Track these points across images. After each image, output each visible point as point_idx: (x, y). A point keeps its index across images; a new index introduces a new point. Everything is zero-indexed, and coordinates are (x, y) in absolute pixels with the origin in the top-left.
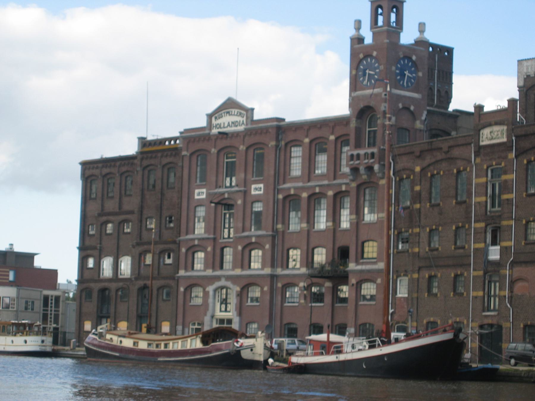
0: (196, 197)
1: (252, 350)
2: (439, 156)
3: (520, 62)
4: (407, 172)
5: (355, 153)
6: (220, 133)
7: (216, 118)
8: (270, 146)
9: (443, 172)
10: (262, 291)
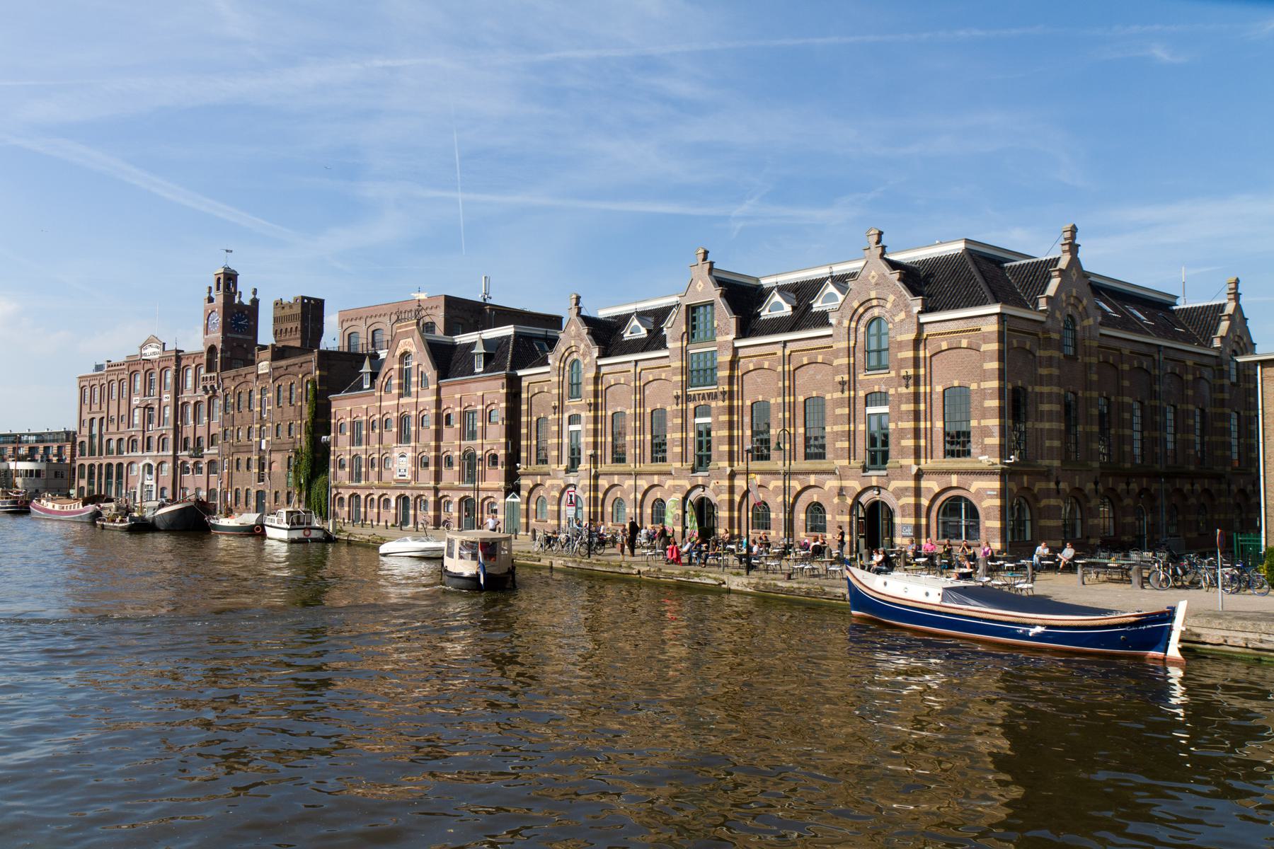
2: (242, 379)
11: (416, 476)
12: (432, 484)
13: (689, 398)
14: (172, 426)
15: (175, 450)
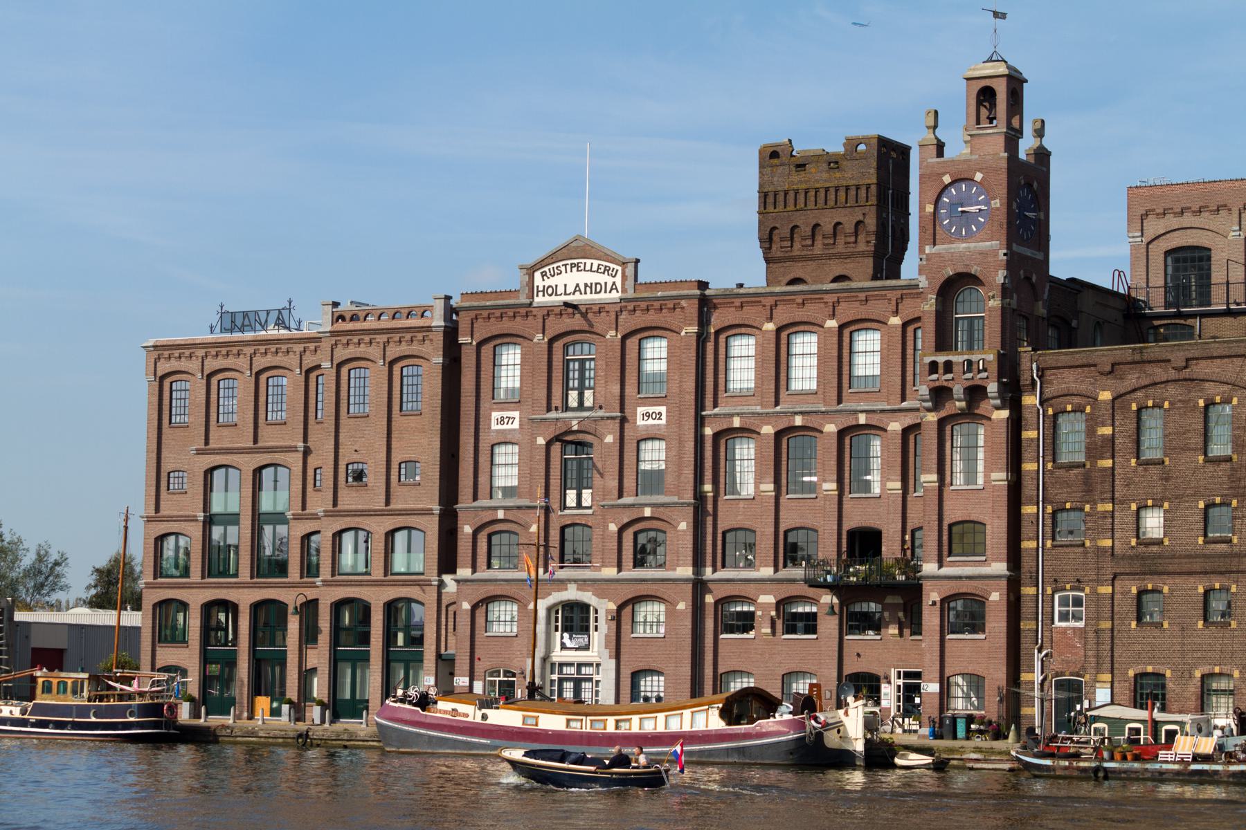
0: (494, 426)
1: (839, 731)
3: (772, 156)
4: (1076, 400)
5: (941, 359)
6: (566, 304)
7: (543, 275)
8: (683, 333)
9: (1170, 403)
10: (671, 613)
14: (689, 497)
15: (698, 563)
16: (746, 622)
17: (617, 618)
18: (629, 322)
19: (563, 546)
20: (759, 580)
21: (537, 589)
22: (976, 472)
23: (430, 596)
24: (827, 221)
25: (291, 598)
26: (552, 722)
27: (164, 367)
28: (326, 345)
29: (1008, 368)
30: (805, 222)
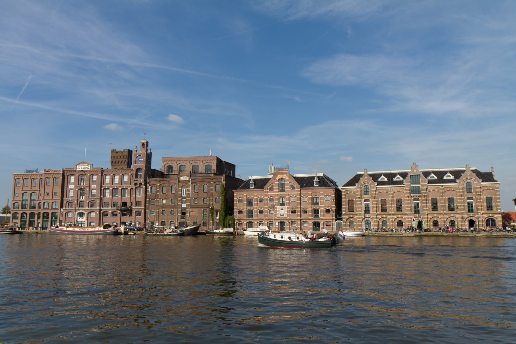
11: (289, 215)
12: (299, 218)
13: (412, 197)
14: (99, 198)
15: (100, 207)
16: (107, 215)
17: (88, 214)
18: (91, 173)
19: (81, 204)
20: (109, 209)
21: (76, 210)
22: (140, 195)
23: (59, 212)
24: (120, 160)
25: (36, 212)
26: (77, 229)
27: (16, 178)
28: (43, 175)
29: (145, 181)
30: (117, 160)
